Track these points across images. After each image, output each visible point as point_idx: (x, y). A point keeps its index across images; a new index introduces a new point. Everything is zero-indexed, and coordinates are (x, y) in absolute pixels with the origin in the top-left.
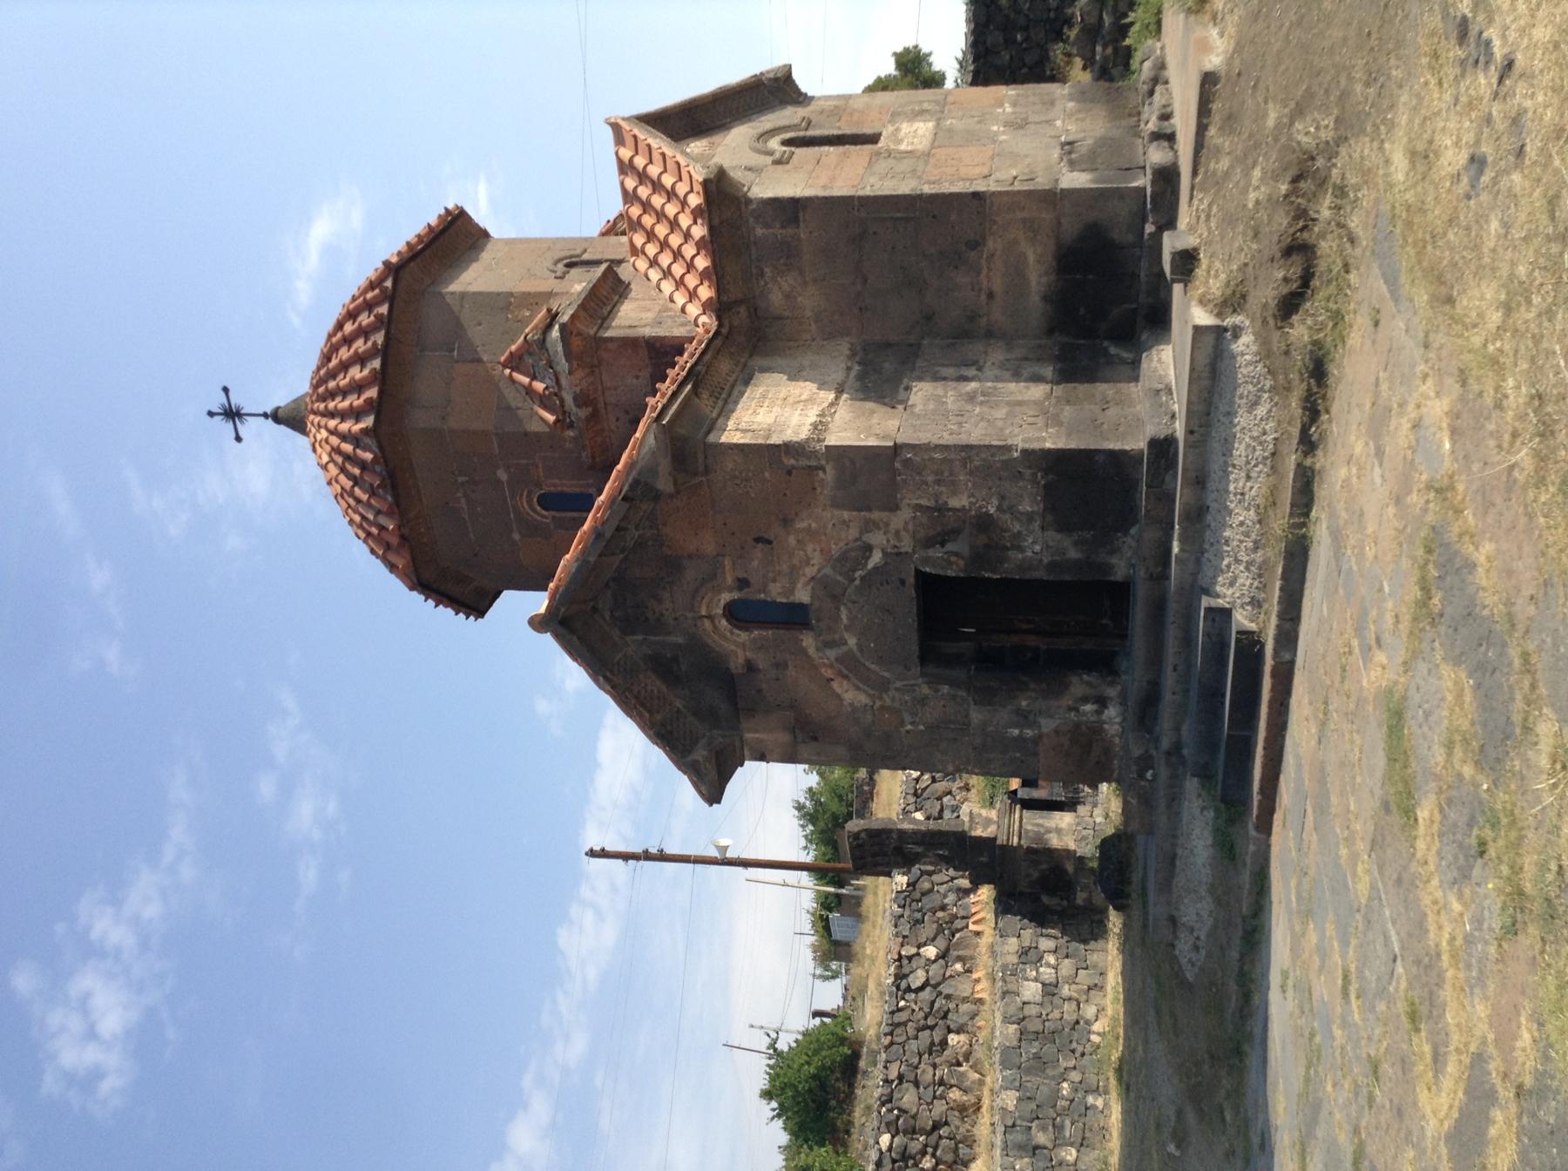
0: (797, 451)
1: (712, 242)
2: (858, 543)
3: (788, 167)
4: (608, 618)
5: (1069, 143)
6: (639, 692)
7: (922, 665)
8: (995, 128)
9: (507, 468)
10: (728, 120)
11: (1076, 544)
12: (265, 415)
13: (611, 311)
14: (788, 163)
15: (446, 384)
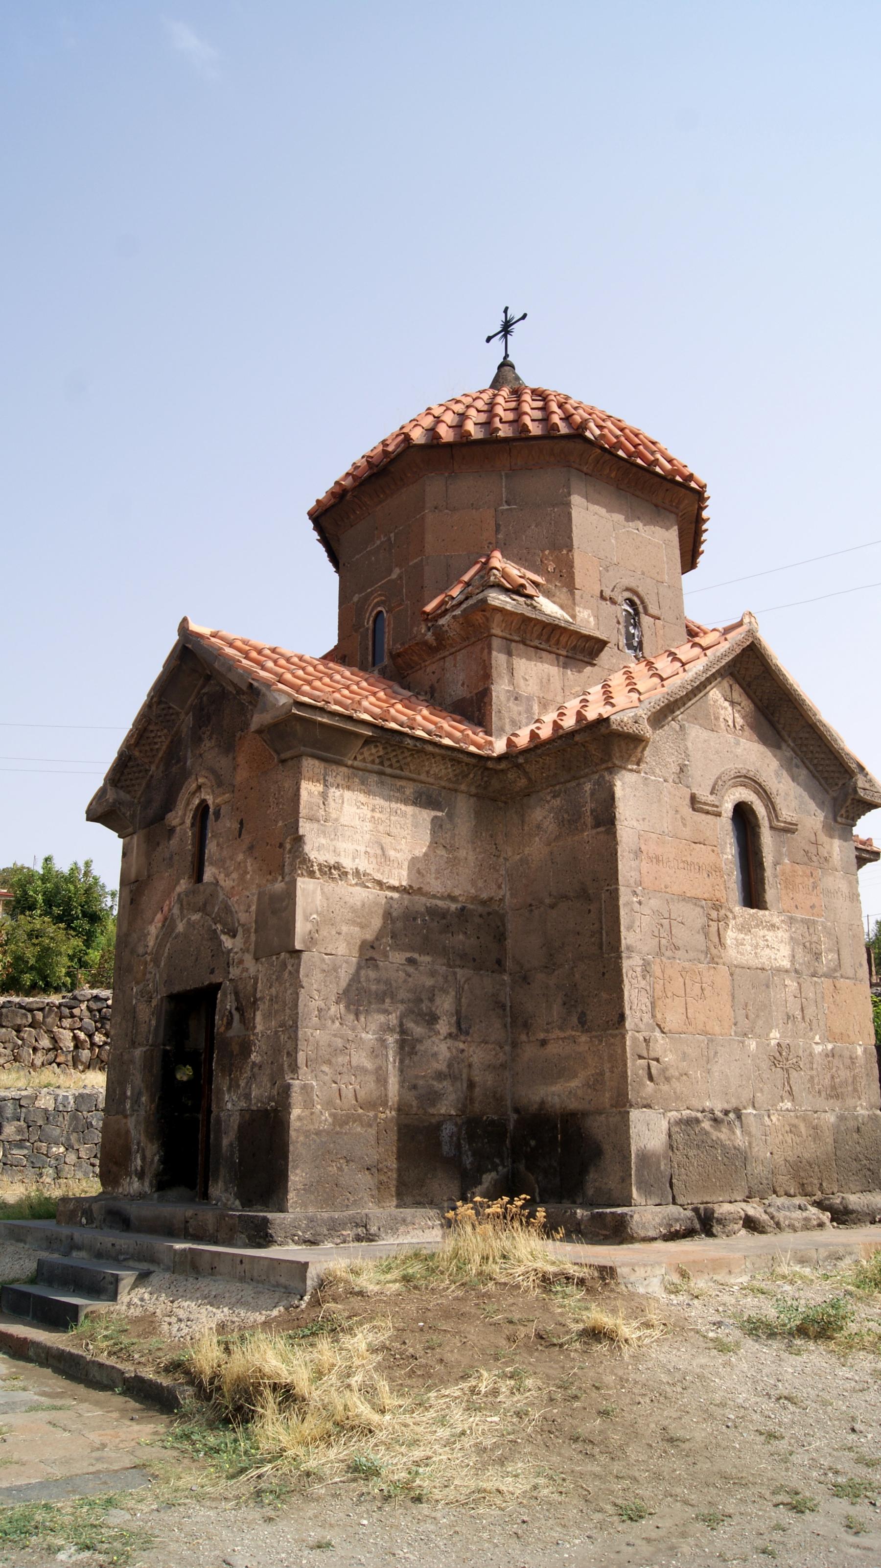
0: (296, 852)
1: (561, 737)
2: (237, 925)
3: (687, 810)
4: (203, 691)
5: (739, 1117)
6: (152, 731)
7: (167, 996)
8: (775, 1034)
9: (400, 577)
10: (792, 744)
11: (231, 1145)
12: (507, 356)
13: (537, 648)
14: (694, 809)
15: (472, 504)
